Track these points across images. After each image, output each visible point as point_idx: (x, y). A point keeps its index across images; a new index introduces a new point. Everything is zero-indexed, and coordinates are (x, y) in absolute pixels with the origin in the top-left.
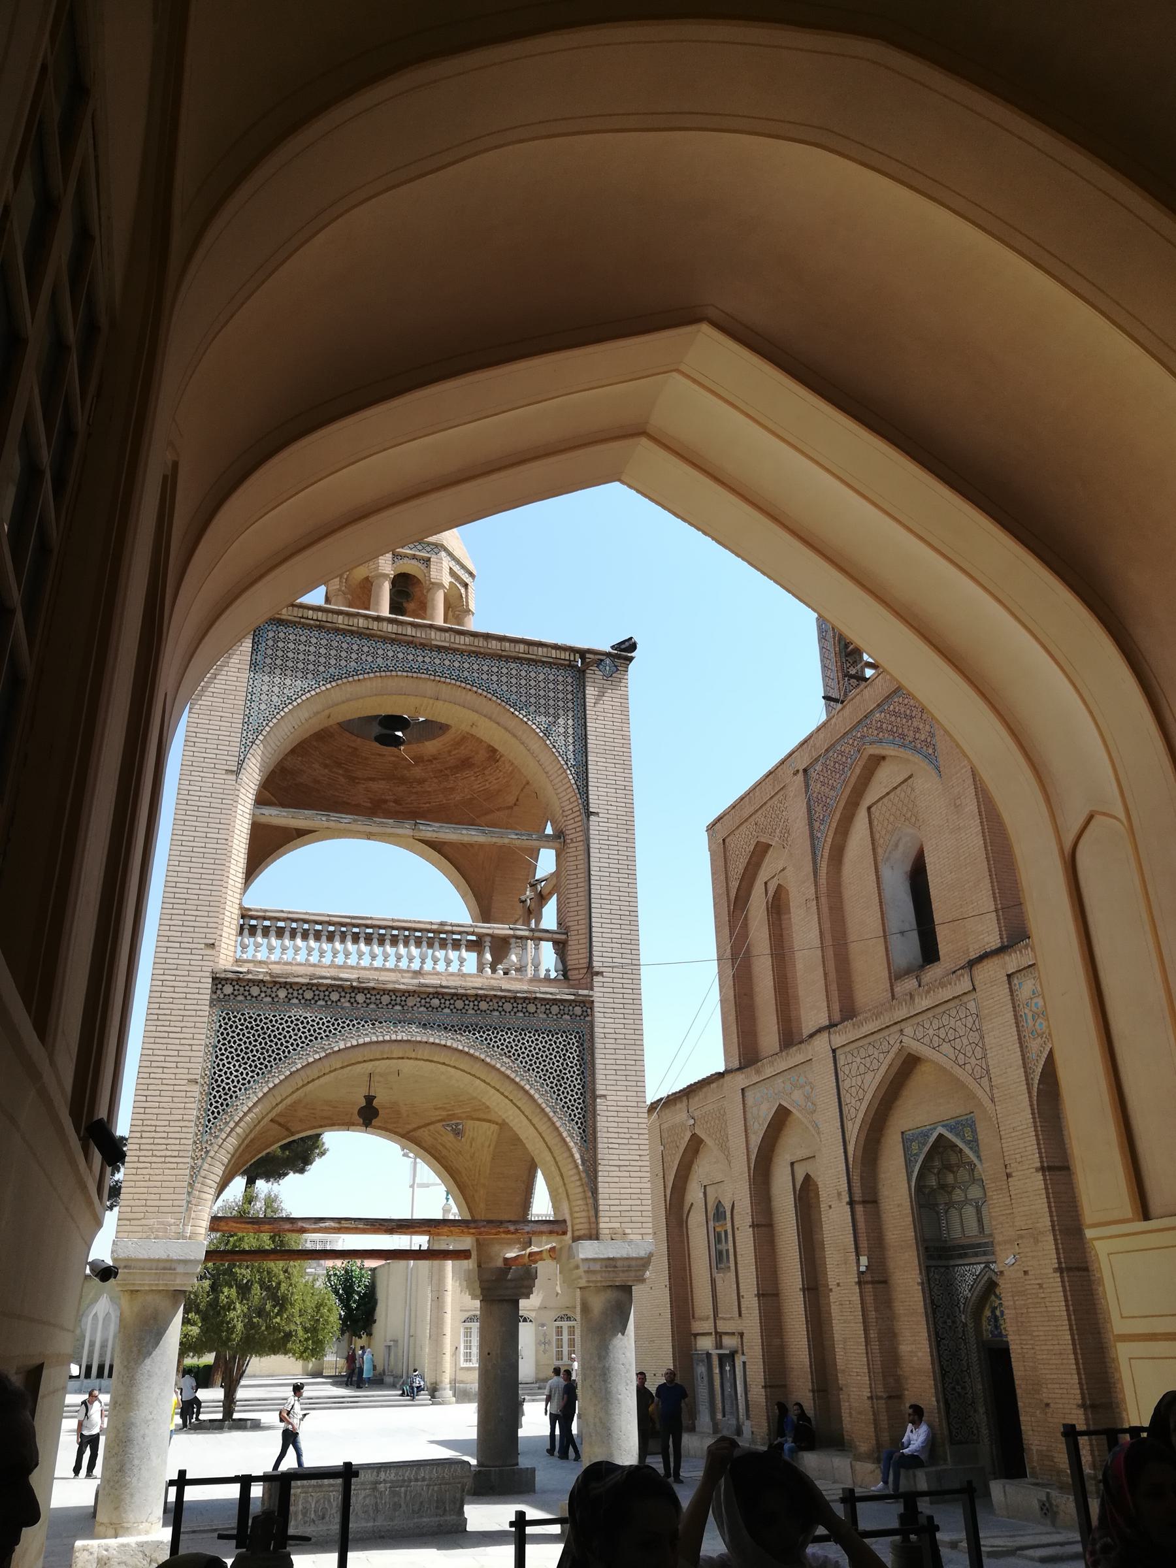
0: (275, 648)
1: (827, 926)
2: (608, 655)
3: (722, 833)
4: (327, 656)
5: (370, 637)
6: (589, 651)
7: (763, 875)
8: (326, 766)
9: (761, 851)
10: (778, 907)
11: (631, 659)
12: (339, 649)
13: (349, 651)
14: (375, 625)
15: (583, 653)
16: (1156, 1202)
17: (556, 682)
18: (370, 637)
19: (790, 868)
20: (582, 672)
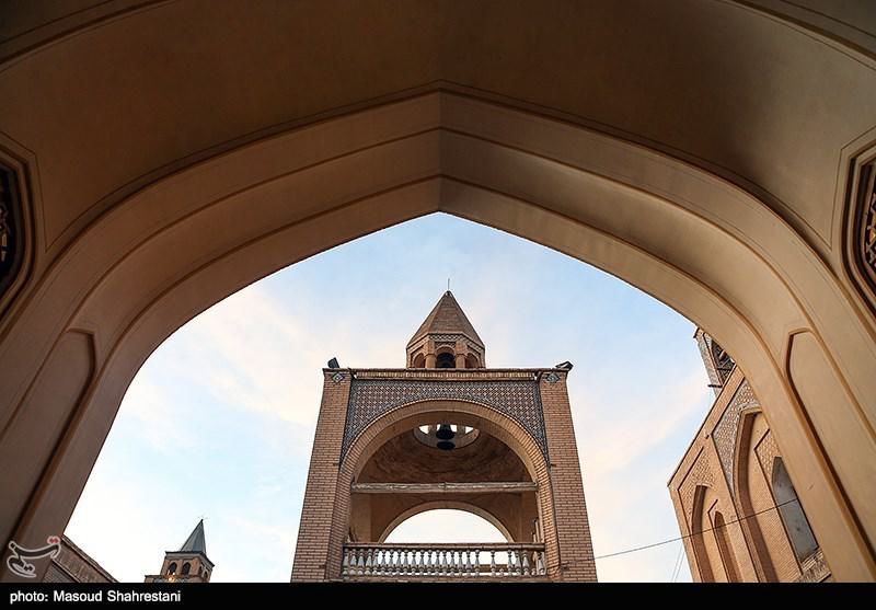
0: (362, 395)
1: (748, 532)
2: (552, 371)
3: (677, 483)
4: (389, 396)
5: (413, 381)
6: (540, 370)
7: (707, 508)
8: (417, 467)
9: (701, 492)
10: (719, 523)
11: (567, 372)
12: (396, 391)
13: (402, 390)
14: (415, 375)
15: (536, 372)
16: (81, 341)
17: (522, 391)
18: (413, 381)
19: (720, 500)
20: (538, 382)
